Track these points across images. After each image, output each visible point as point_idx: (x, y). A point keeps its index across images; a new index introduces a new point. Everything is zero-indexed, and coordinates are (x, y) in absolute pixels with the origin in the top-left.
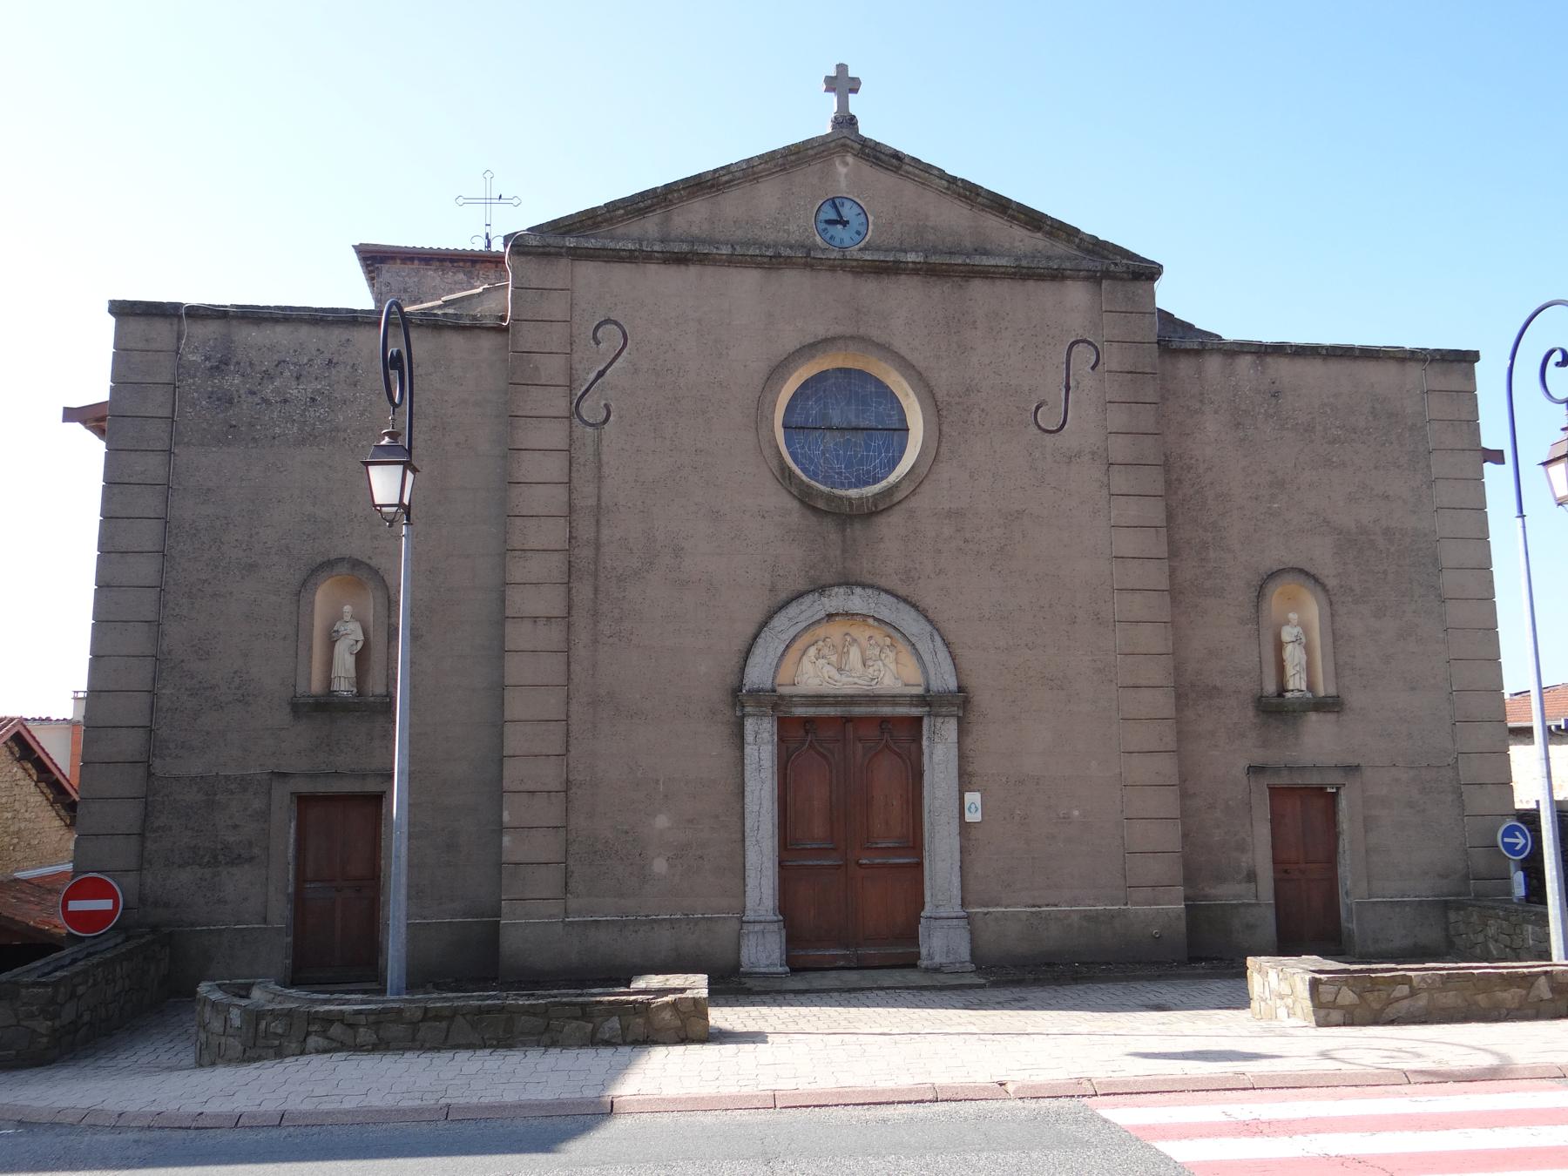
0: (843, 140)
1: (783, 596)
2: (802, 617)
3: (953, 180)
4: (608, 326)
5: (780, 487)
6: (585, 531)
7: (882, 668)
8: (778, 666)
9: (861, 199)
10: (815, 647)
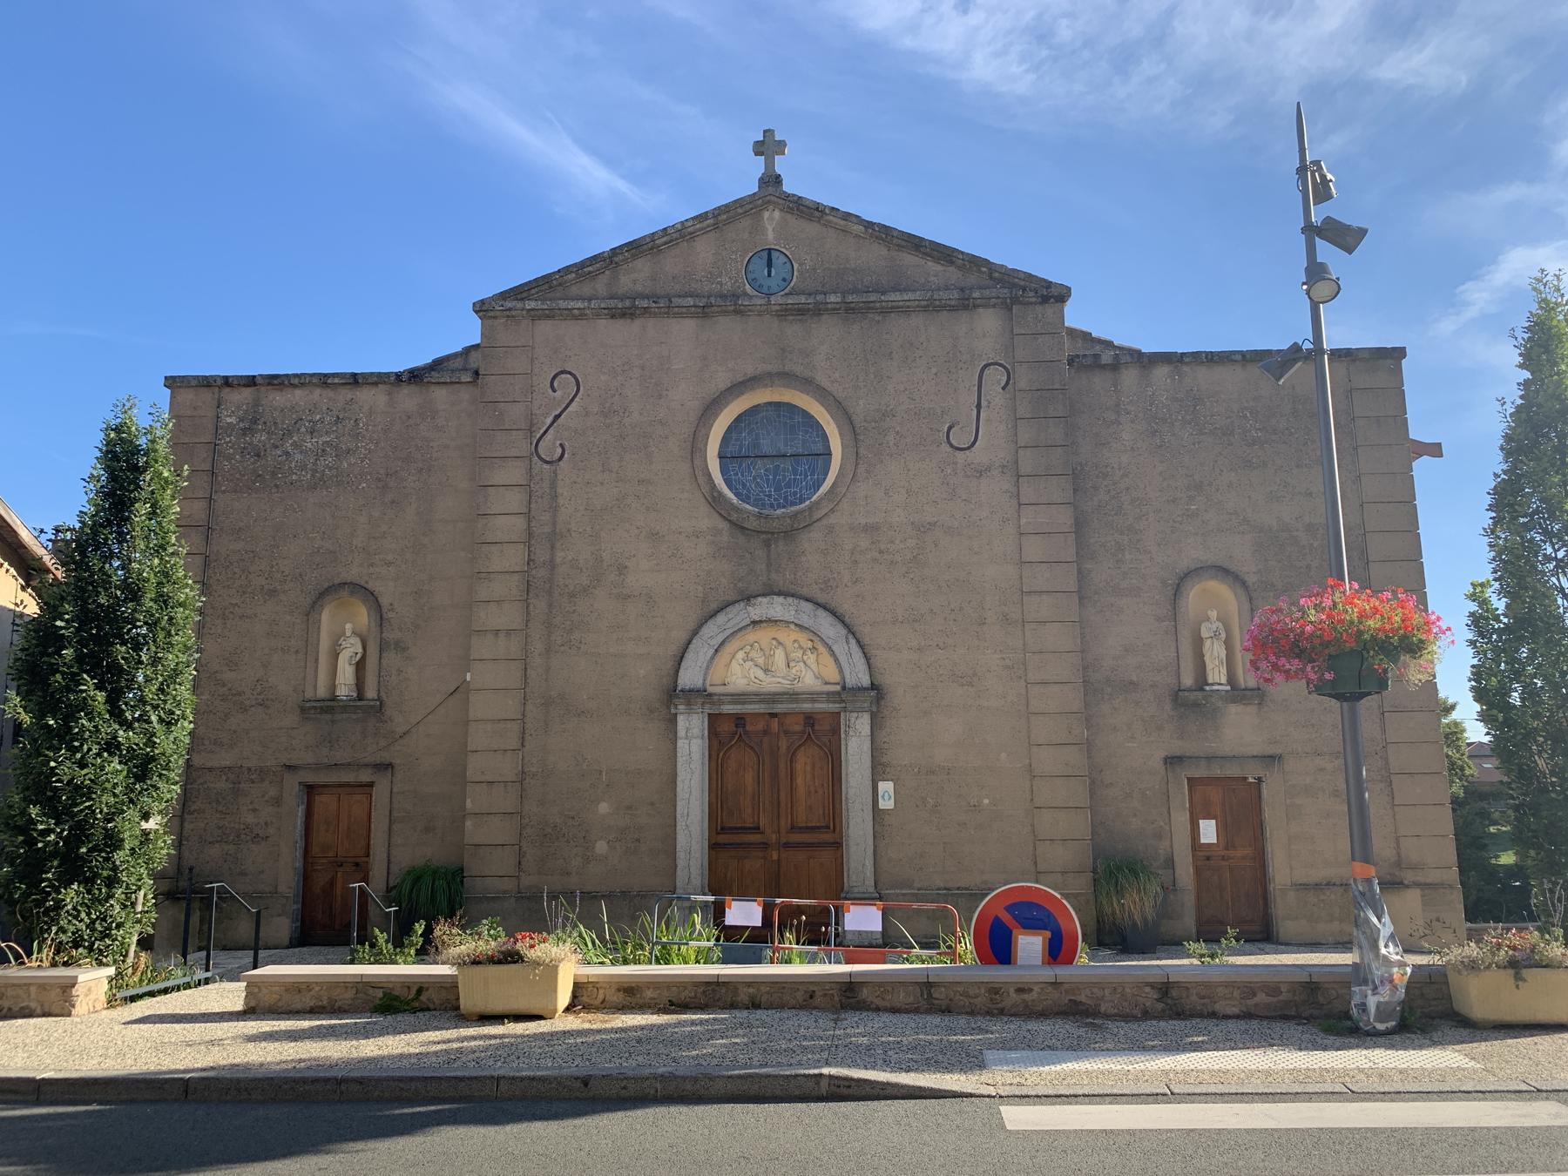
0: (768, 198)
1: (714, 606)
2: (729, 625)
3: (869, 225)
4: (563, 376)
5: (712, 510)
6: (542, 555)
7: (803, 669)
8: (708, 668)
9: (786, 249)
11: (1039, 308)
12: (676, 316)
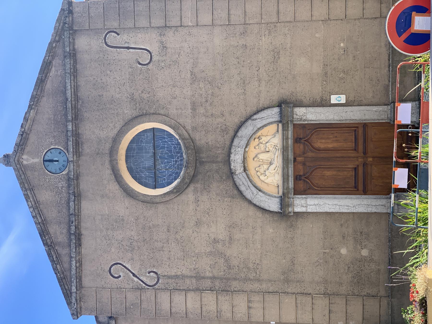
0: (16, 161)
1: (236, 192)
2: (246, 184)
4: (112, 272)
5: (184, 192)
6: (208, 283)
7: (270, 144)
8: (269, 195)
9: (43, 152)
10: (260, 176)
11: (75, 15)
12: (79, 209)
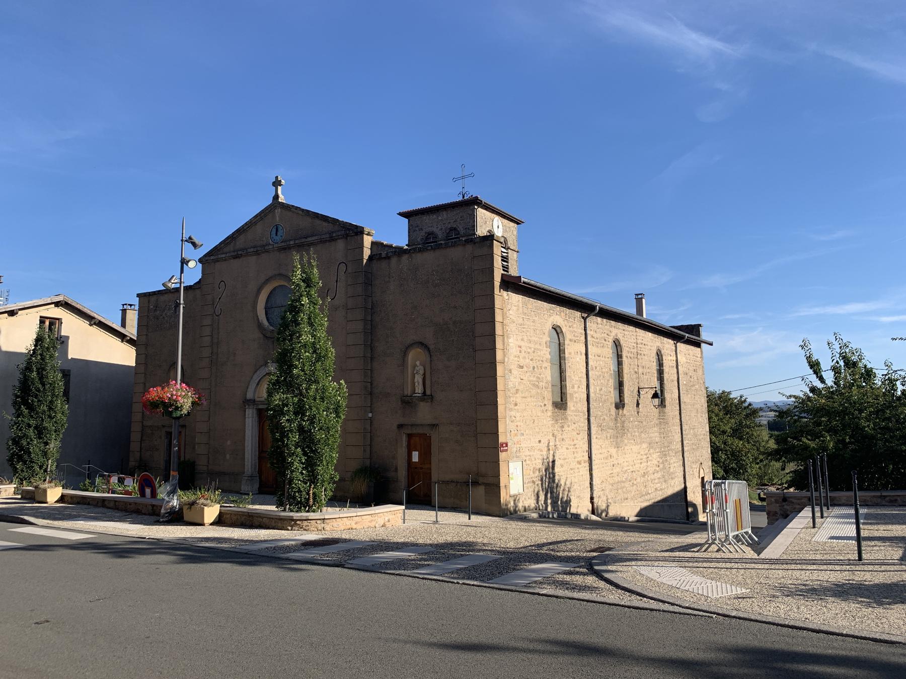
3: (303, 210)
11: (356, 237)
12: (251, 255)
